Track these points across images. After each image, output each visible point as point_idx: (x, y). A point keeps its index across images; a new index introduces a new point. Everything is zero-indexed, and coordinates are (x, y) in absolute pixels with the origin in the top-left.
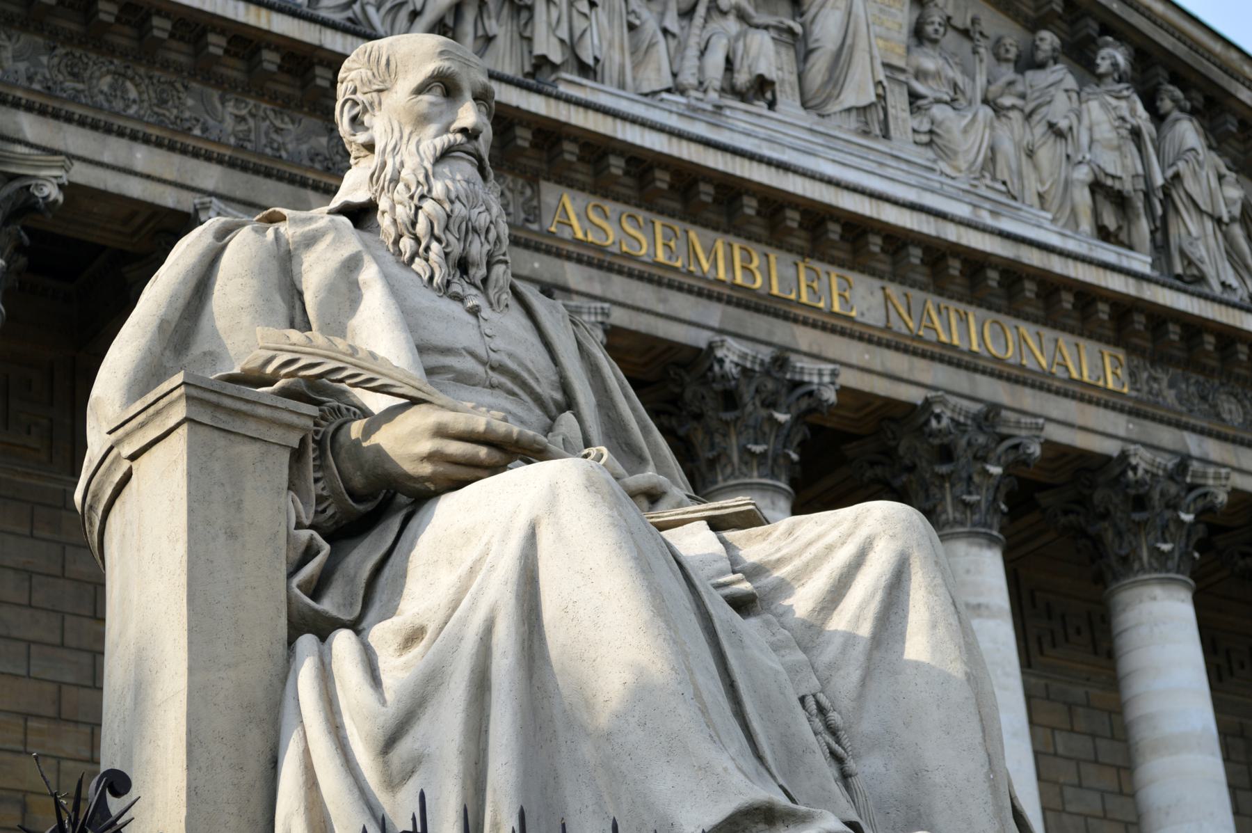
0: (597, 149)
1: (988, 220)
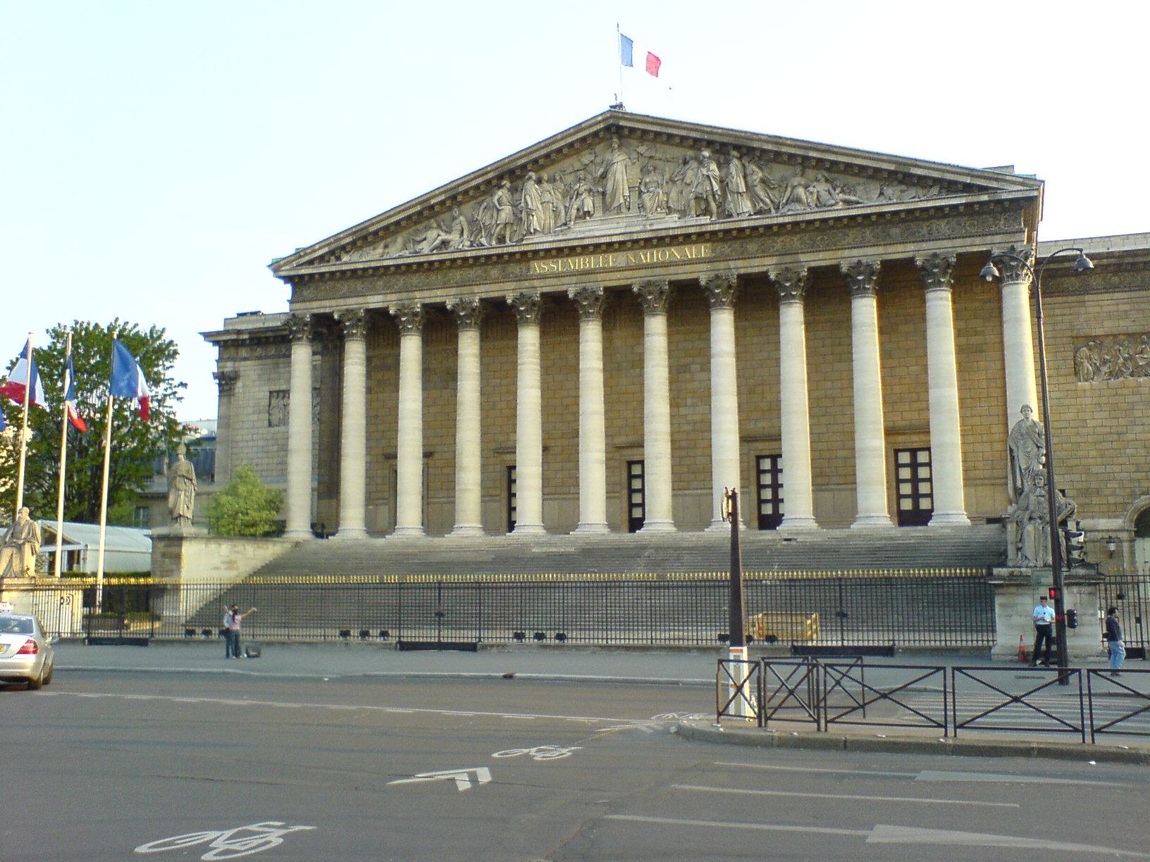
0: (536, 252)
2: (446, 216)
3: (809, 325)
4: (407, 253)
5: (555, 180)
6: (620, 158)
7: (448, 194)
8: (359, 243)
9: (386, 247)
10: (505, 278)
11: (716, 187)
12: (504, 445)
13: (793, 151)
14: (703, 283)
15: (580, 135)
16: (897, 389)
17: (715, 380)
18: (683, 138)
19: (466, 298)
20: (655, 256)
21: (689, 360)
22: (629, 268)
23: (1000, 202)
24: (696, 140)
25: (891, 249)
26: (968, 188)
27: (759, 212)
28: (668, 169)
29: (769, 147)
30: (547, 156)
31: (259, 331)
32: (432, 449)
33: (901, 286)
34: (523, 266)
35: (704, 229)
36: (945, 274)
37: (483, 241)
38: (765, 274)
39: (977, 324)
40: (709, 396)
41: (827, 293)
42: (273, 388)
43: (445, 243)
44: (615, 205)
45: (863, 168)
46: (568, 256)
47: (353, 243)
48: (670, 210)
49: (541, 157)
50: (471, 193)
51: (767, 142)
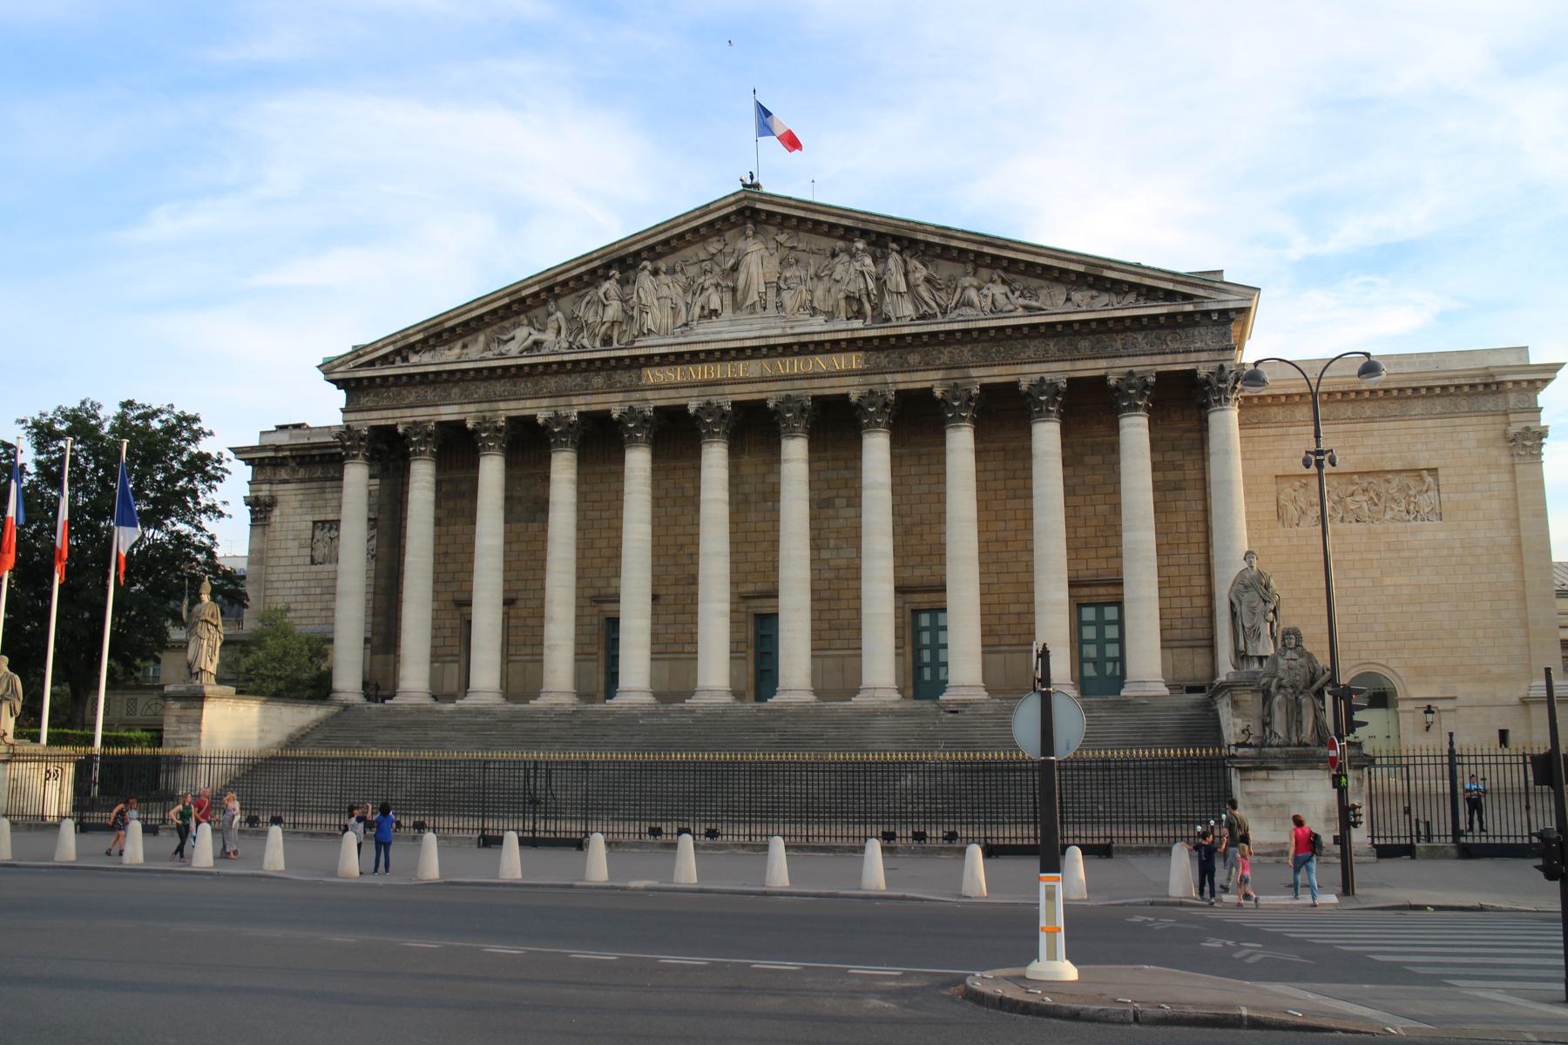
0: (649, 357)
1: (789, 331)
2: (540, 312)
3: (979, 454)
4: (489, 354)
5: (675, 272)
6: (755, 247)
7: (544, 285)
8: (431, 342)
9: (465, 346)
10: (610, 388)
11: (871, 285)
12: (603, 592)
13: (964, 245)
14: (854, 398)
15: (707, 219)
16: (1081, 532)
17: (867, 518)
18: (832, 226)
19: (563, 412)
20: (796, 365)
21: (832, 493)
22: (763, 380)
23: (1207, 313)
24: (847, 228)
25: (1079, 365)
26: (1170, 296)
27: (923, 317)
28: (814, 263)
29: (936, 240)
30: (666, 242)
31: (304, 447)
32: (513, 595)
33: (1090, 411)
34: (633, 373)
35: (856, 335)
36: (1142, 396)
37: (586, 342)
38: (929, 391)
39: (1176, 456)
40: (858, 537)
41: (1002, 416)
42: (317, 518)
43: (537, 344)
44: (749, 302)
45: (1047, 269)
46: (689, 363)
47: (424, 341)
48: (814, 311)
49: (658, 243)
50: (571, 284)
51: (932, 233)
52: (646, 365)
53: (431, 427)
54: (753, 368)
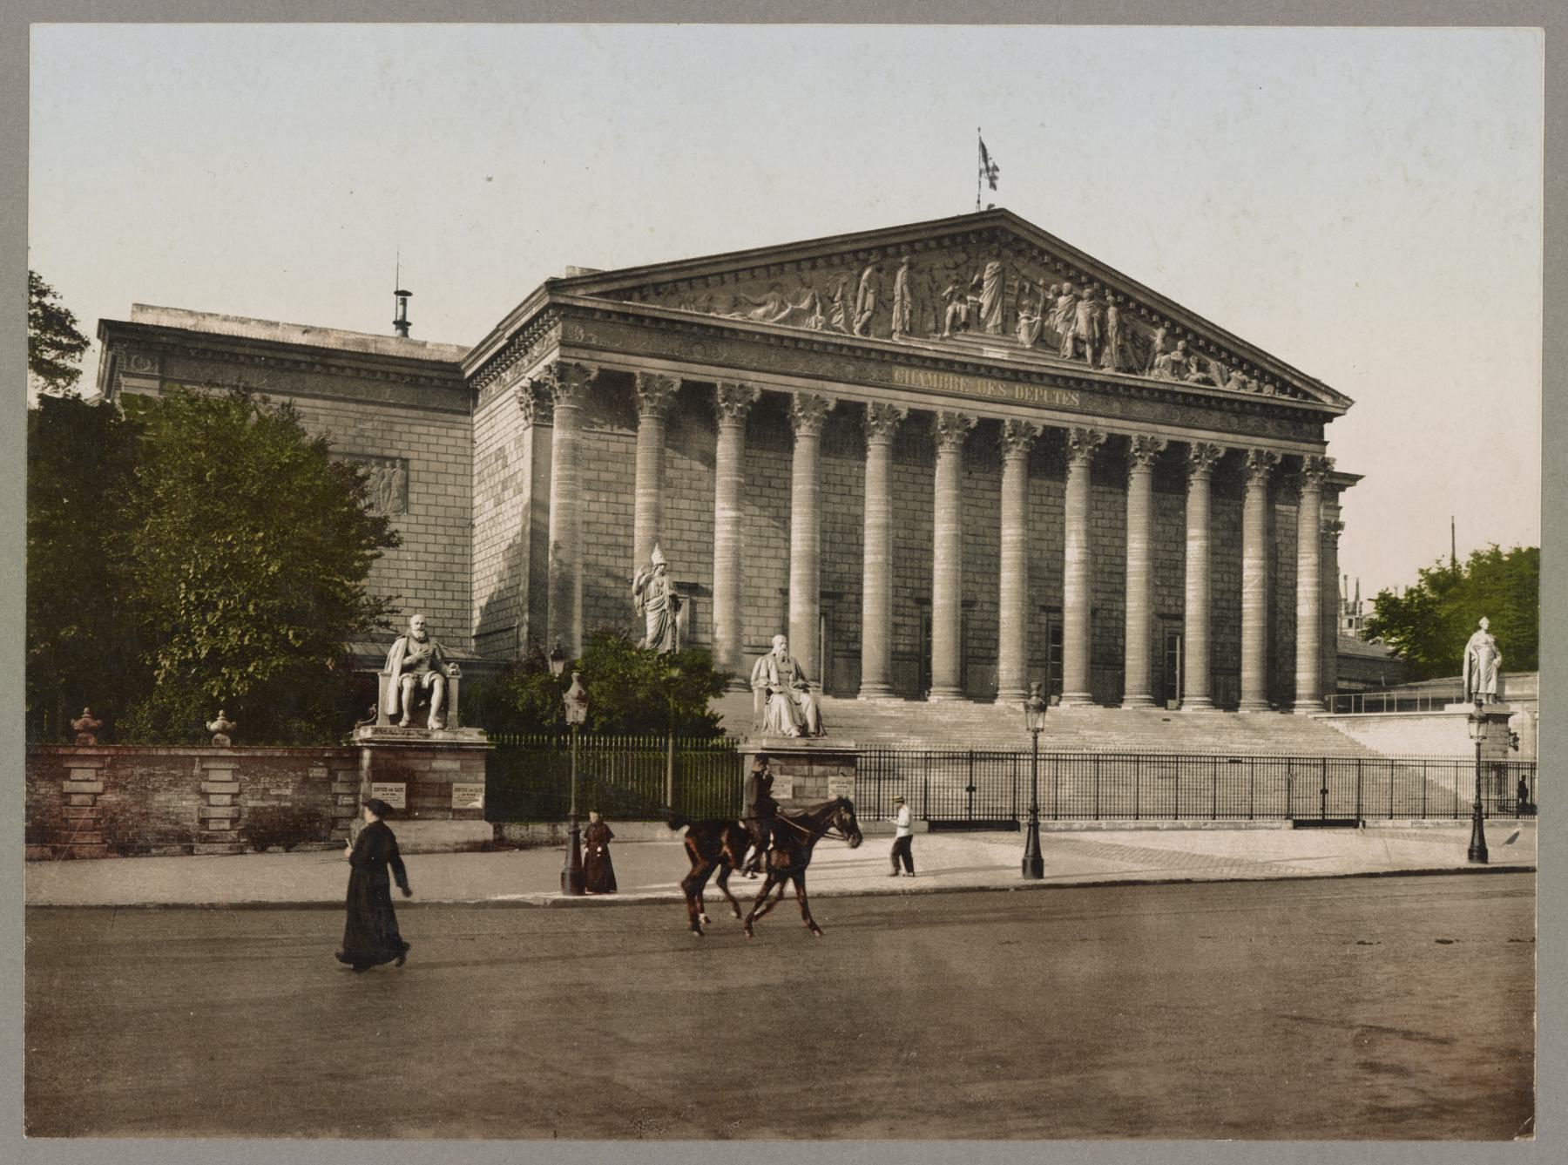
23: (1316, 412)
26: (1295, 391)
52: (900, 364)
53: (677, 386)
54: (988, 387)
